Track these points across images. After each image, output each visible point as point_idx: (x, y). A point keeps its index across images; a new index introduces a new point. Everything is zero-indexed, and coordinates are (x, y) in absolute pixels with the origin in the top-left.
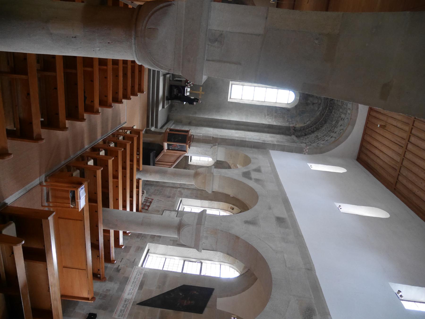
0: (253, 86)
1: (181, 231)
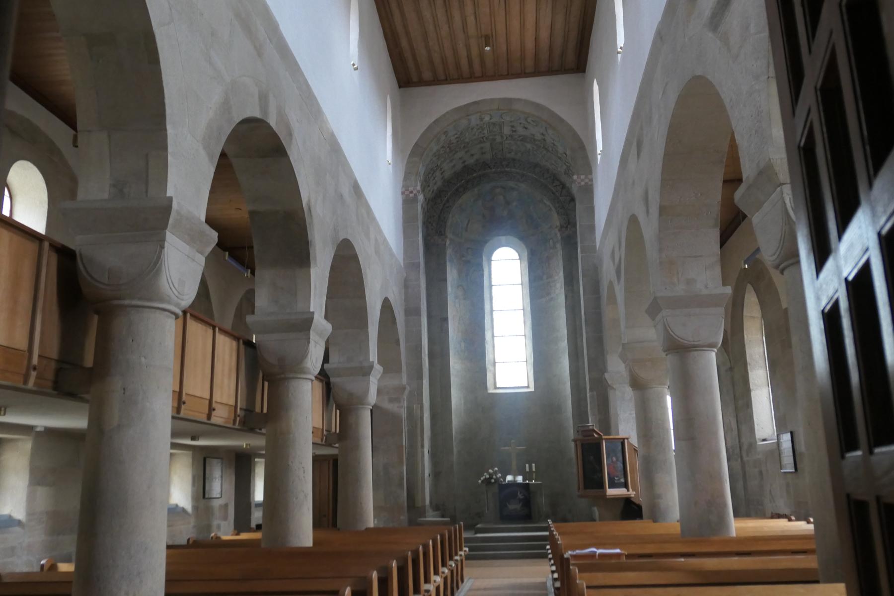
1: (690, 343)
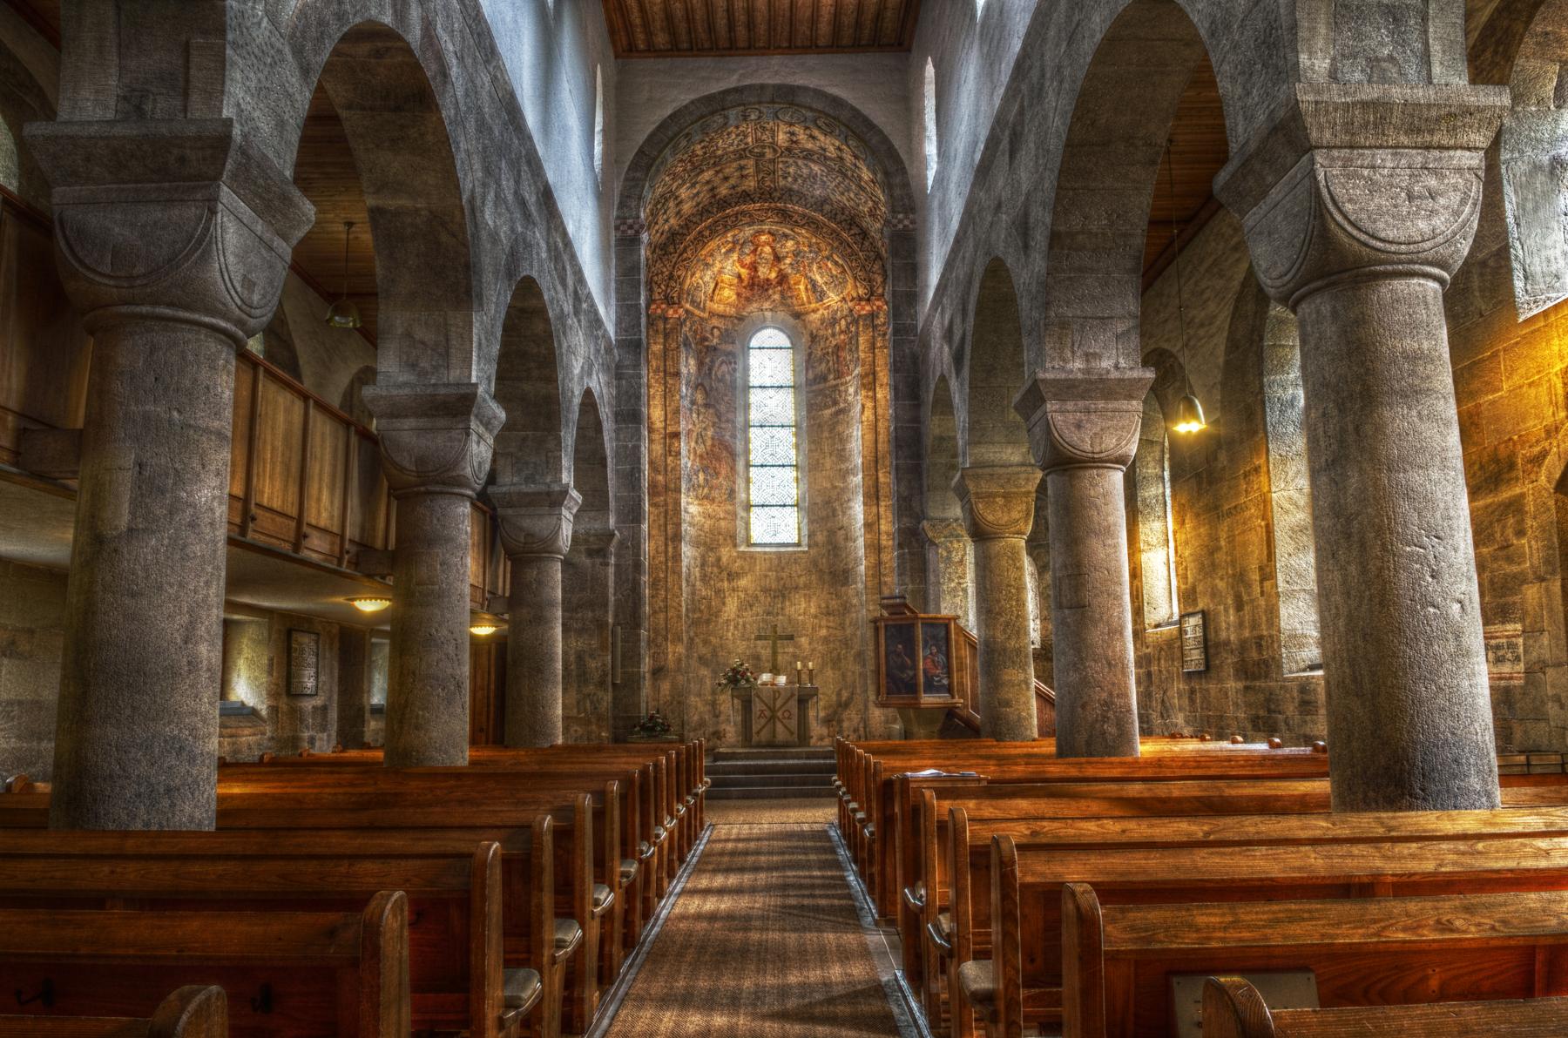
0: (748, 472)
